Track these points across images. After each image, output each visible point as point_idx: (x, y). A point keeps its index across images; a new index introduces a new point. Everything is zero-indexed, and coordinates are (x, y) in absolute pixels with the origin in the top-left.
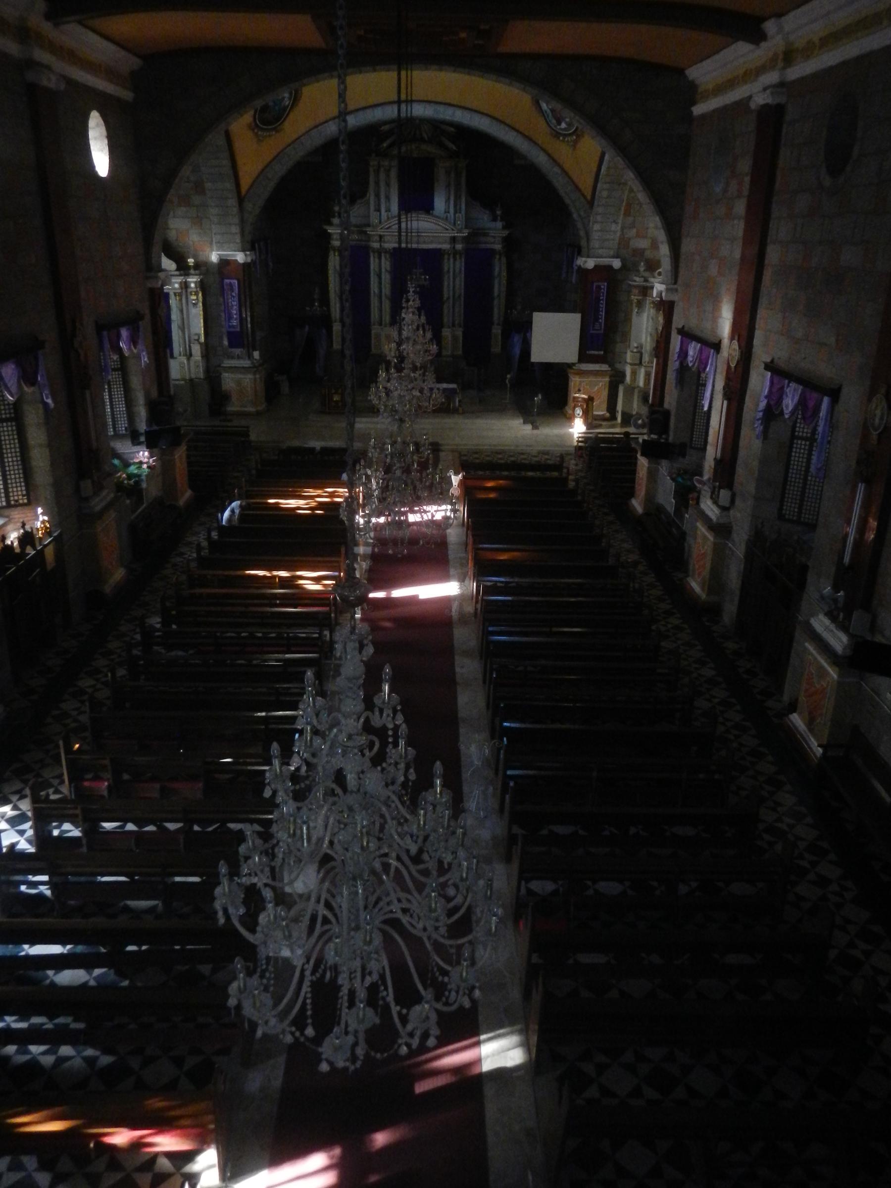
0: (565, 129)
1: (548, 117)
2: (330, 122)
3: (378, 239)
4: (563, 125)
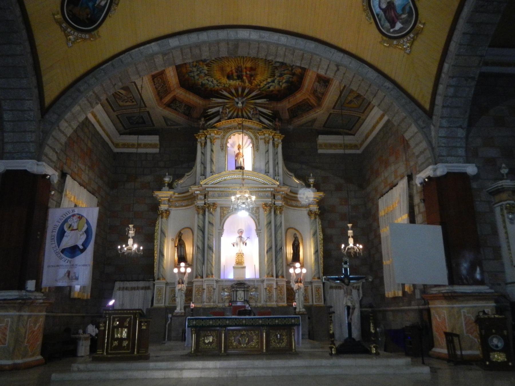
0: (401, 30)
1: (380, 20)
2: (153, 44)
3: (202, 197)
4: (399, 26)
